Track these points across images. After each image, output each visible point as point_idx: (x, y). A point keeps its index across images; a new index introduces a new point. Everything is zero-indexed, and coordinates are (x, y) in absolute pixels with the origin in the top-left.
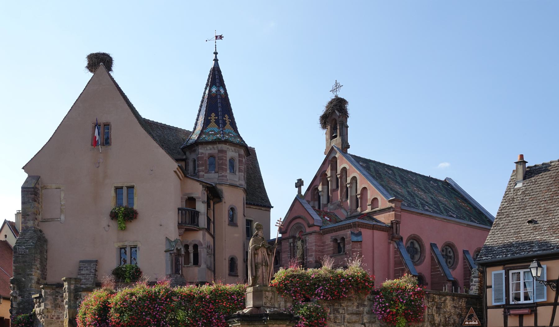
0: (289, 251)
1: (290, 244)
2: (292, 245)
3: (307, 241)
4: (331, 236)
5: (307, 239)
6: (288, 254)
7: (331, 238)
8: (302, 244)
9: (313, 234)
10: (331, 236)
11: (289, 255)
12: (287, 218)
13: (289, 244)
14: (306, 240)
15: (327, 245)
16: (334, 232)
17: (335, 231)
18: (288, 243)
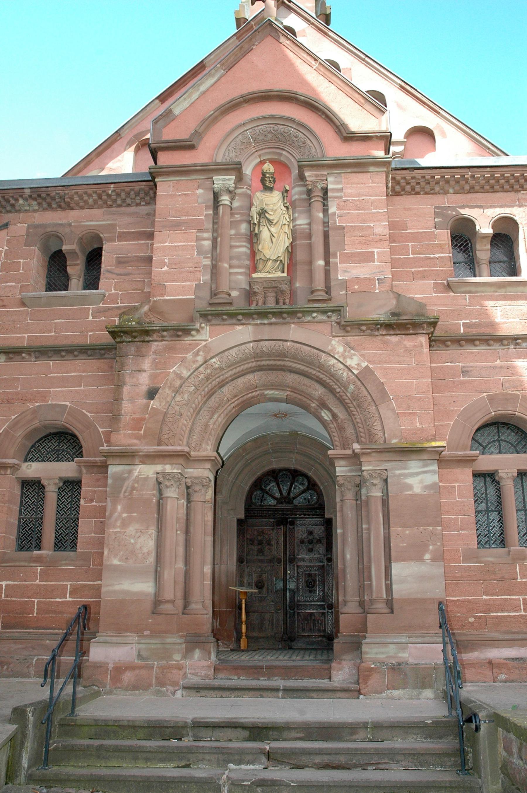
0: (209, 225)
1: (216, 196)
2: (225, 199)
3: (330, 194)
4: (436, 207)
5: (330, 187)
6: (198, 239)
7: (436, 215)
8: (287, 208)
9: (371, 169)
10: (436, 207)
11: (207, 244)
12: (204, 93)
13: (212, 196)
14: (325, 191)
15: (415, 237)
16: (455, 193)
17: (467, 187)
18: (200, 191)
